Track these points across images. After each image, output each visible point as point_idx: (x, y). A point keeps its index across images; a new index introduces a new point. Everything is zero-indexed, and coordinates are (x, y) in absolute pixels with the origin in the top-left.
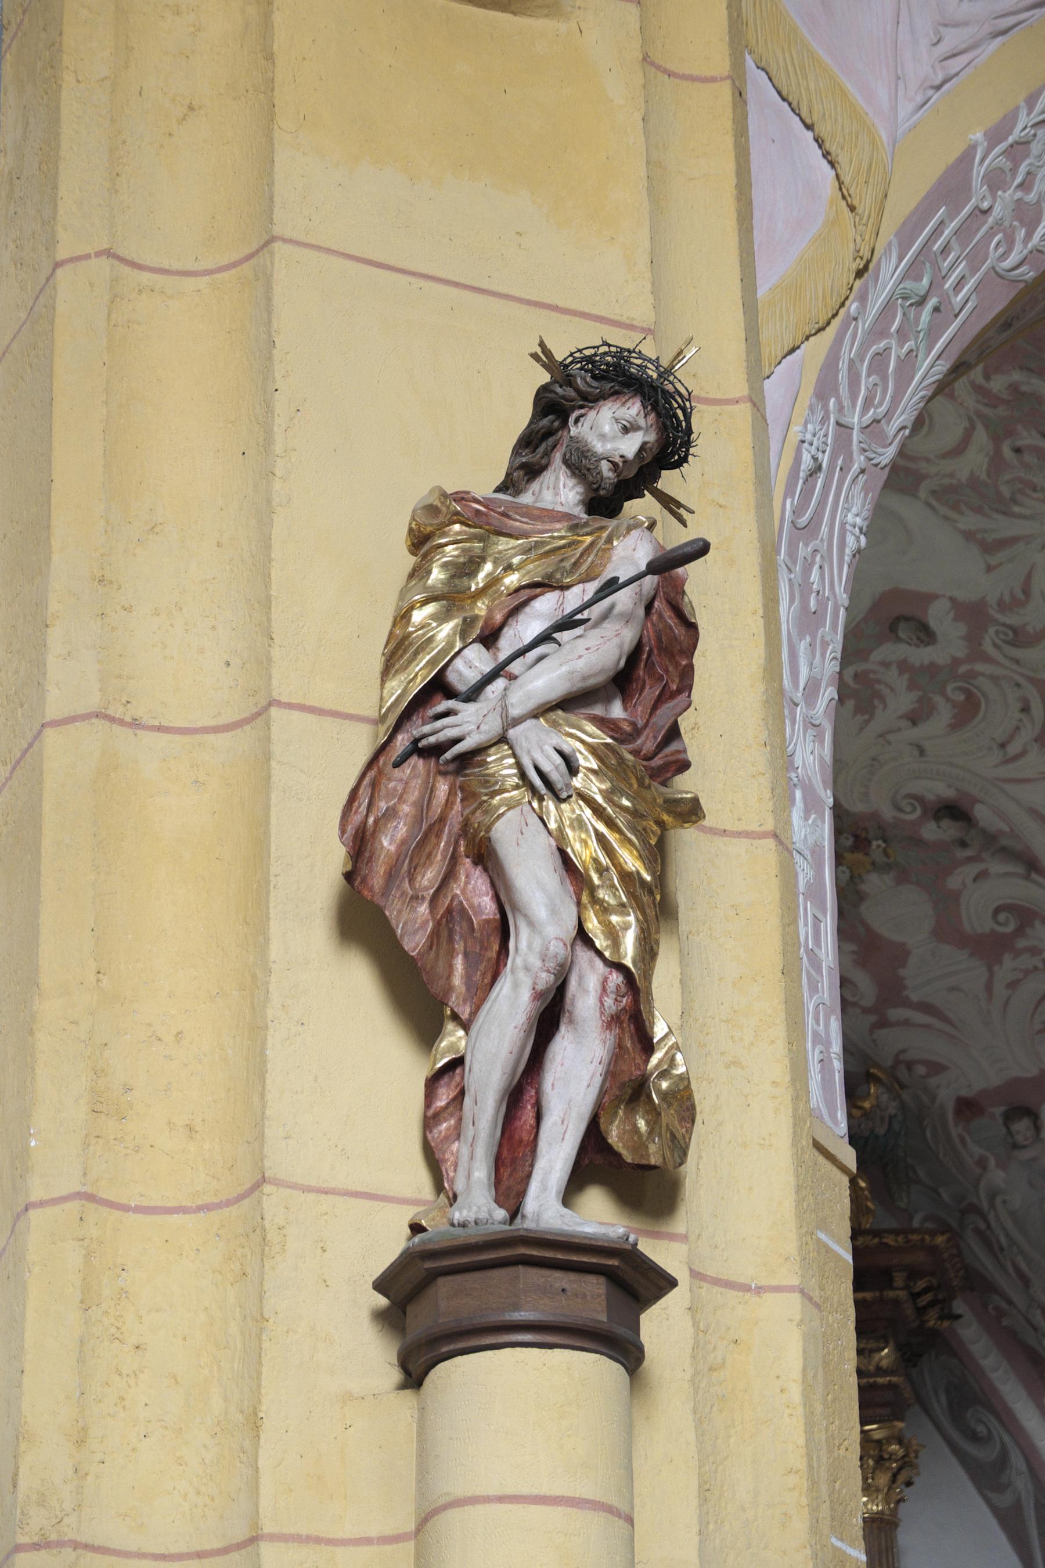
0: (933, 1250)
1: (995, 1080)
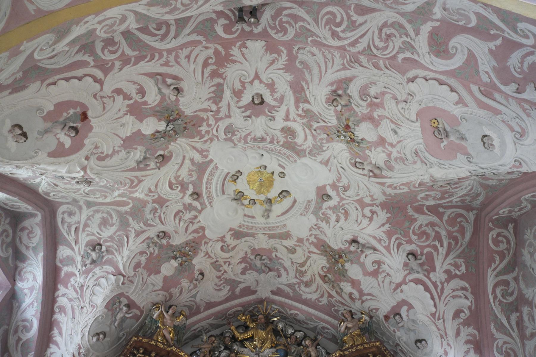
0: (377, 347)
1: (389, 309)
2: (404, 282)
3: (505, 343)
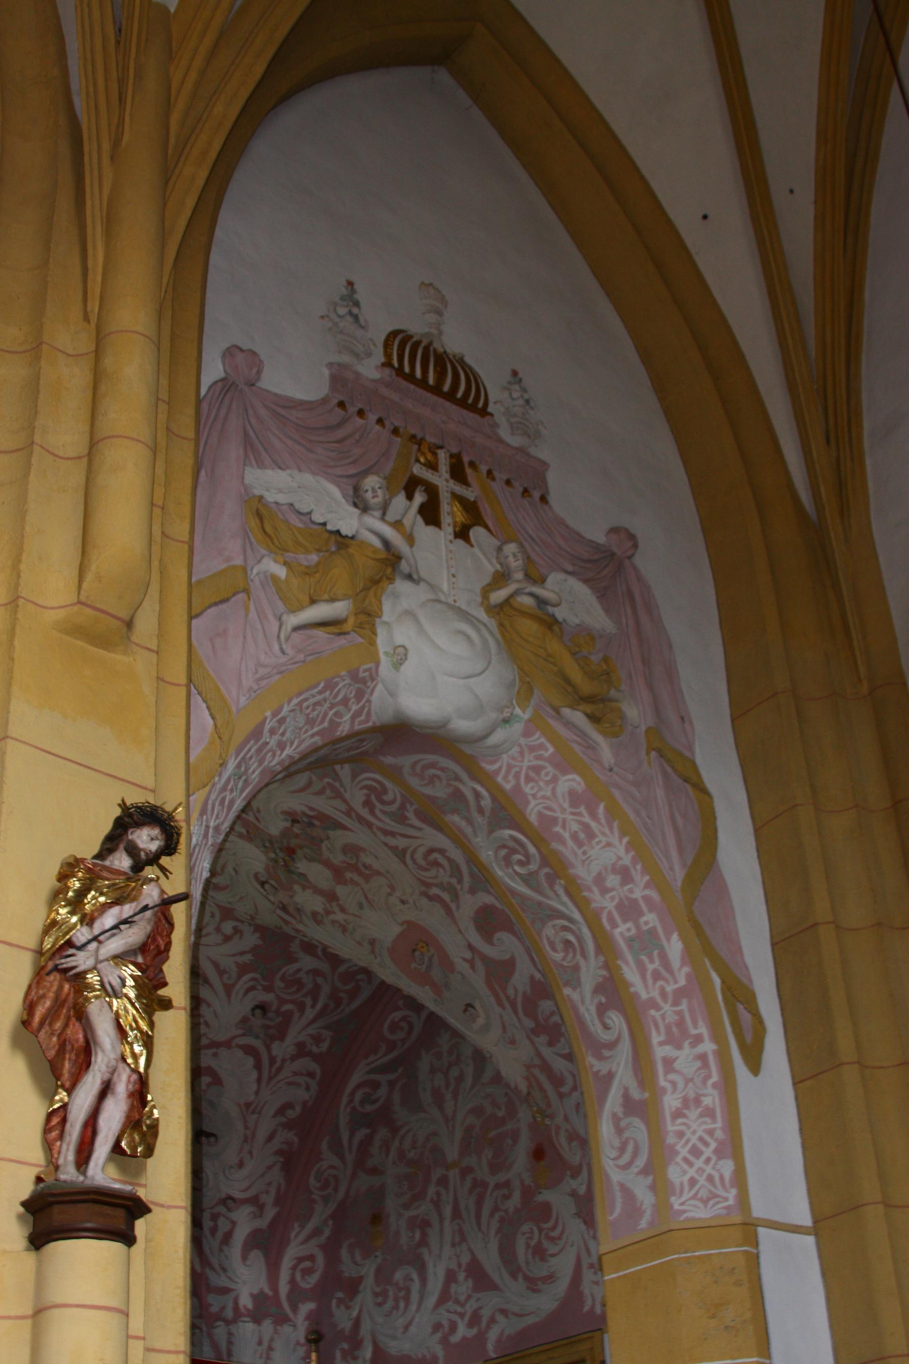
2: (227, 1044)
3: (332, 1167)
